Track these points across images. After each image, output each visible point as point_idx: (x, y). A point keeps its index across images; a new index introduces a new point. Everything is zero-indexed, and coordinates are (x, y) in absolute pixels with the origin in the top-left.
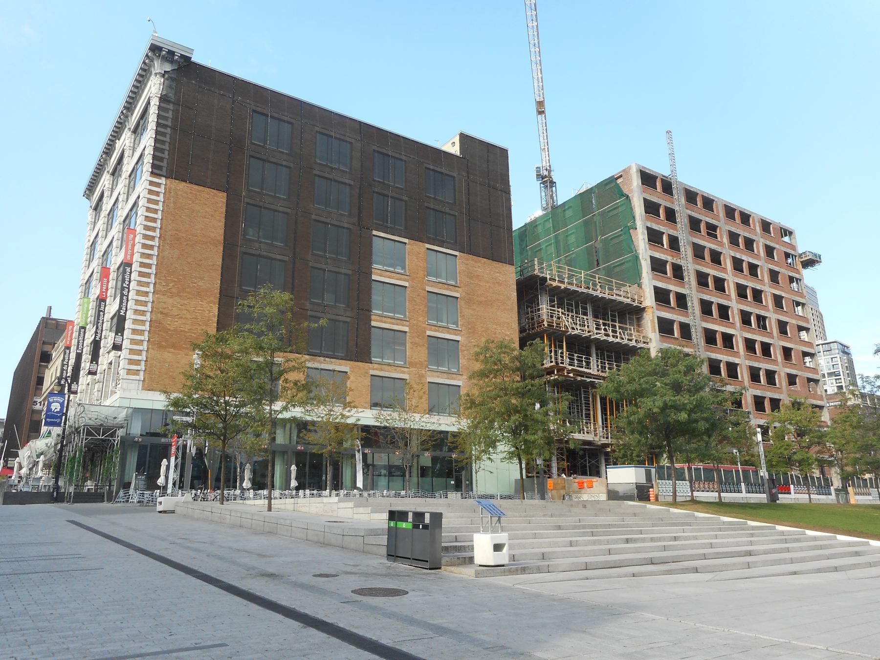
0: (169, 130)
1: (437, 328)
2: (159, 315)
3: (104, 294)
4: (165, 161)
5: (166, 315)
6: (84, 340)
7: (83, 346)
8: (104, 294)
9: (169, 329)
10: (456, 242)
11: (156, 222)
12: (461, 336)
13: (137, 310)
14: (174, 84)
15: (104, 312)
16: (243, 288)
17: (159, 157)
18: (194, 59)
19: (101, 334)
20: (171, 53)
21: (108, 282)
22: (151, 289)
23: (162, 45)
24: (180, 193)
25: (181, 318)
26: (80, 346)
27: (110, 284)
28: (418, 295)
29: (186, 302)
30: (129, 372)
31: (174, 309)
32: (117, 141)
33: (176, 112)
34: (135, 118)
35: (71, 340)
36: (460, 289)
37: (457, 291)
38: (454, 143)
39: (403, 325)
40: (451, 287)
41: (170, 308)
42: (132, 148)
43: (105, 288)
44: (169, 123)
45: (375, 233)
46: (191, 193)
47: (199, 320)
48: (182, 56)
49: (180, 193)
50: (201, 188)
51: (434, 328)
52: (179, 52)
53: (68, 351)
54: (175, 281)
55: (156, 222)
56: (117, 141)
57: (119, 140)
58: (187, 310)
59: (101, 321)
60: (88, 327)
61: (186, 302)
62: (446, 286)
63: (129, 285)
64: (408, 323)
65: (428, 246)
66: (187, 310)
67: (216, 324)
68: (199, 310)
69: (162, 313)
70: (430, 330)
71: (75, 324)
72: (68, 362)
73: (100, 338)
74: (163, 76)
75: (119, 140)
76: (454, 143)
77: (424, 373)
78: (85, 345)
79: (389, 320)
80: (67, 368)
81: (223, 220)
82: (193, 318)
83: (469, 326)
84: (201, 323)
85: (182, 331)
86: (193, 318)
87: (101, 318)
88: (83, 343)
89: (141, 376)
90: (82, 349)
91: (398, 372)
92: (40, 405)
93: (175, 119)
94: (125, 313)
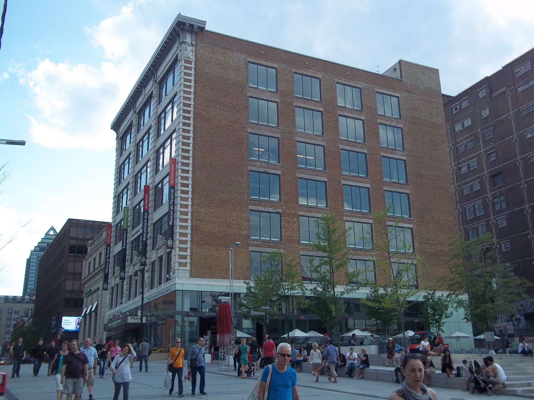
1: (394, 219)
2: (196, 221)
4: (192, 106)
5: (202, 221)
7: (126, 243)
8: (146, 206)
9: (204, 231)
10: (404, 149)
11: (189, 153)
12: (413, 224)
13: (182, 219)
18: (207, 28)
20: (192, 26)
21: (149, 196)
22: (190, 203)
23: (184, 21)
24: (204, 129)
25: (212, 222)
26: (125, 244)
28: (378, 194)
29: (214, 211)
30: (180, 264)
31: (206, 216)
32: (143, 89)
34: (161, 74)
35: (111, 238)
36: (409, 187)
37: (408, 189)
38: (395, 69)
39: (368, 219)
40: (403, 186)
41: (204, 216)
42: (158, 96)
46: (211, 129)
47: (223, 224)
48: (199, 27)
49: (204, 129)
51: (391, 219)
52: (196, 25)
54: (205, 195)
55: (189, 153)
56: (143, 89)
58: (215, 216)
61: (214, 211)
62: (398, 185)
63: (174, 202)
64: (372, 217)
66: (215, 216)
68: (223, 216)
69: (198, 220)
70: (389, 221)
71: (113, 226)
75: (145, 89)
76: (395, 69)
79: (358, 215)
80: (109, 260)
82: (220, 222)
83: (419, 216)
84: (225, 226)
85: (212, 232)
86: (220, 222)
87: (146, 224)
88: (126, 241)
89: (188, 268)
91: (367, 256)
94: (173, 223)
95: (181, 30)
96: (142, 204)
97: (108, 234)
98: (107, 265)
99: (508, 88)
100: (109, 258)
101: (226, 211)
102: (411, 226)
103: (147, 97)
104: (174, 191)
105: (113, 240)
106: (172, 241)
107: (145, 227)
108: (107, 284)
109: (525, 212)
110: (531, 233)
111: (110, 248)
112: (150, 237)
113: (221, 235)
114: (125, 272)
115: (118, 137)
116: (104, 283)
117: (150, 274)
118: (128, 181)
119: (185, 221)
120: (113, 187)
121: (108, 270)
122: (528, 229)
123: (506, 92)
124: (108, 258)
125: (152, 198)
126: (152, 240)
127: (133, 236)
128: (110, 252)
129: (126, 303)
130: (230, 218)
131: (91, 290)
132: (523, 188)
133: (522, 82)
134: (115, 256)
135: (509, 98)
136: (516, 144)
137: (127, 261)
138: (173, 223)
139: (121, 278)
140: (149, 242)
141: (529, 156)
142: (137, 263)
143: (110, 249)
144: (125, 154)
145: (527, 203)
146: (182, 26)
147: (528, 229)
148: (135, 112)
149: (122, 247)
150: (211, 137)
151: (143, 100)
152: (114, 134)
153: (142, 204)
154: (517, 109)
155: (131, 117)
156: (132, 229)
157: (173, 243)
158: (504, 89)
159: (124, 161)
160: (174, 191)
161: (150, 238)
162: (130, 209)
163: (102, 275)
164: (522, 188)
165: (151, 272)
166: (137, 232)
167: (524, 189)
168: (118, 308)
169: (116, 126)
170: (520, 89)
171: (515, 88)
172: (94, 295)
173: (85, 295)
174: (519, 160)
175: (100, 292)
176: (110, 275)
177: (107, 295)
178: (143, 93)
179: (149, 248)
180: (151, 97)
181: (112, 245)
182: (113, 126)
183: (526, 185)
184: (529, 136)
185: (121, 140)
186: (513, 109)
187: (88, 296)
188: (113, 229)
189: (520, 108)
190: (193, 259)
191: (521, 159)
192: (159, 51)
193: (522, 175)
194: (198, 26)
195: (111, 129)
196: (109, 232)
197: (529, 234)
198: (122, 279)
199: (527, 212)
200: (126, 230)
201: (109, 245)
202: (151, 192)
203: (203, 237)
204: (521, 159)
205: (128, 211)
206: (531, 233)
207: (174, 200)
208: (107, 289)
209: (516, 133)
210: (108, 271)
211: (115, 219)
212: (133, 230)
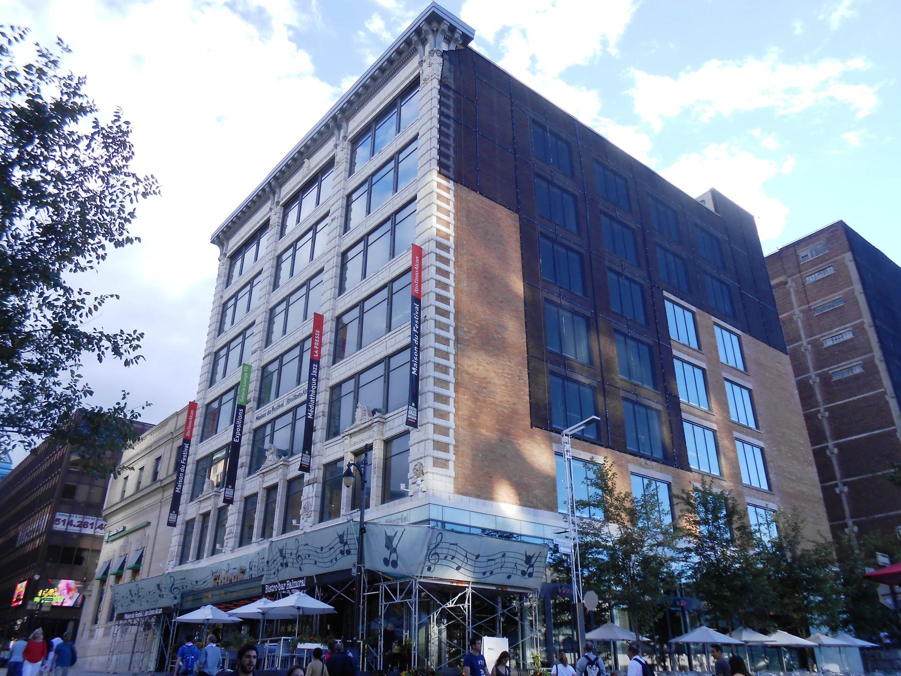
0: (451, 122)
3: (316, 352)
6: (242, 424)
7: (241, 432)
8: (316, 352)
14: (453, 69)
15: (317, 378)
16: (549, 348)
17: (444, 153)
19: (314, 409)
20: (452, 29)
27: (324, 338)
31: (481, 368)
32: (306, 160)
33: (457, 102)
35: (192, 427)
37: (749, 381)
43: (317, 344)
44: (451, 113)
45: (666, 294)
46: (482, 207)
50: (492, 203)
53: (187, 446)
56: (306, 160)
57: (308, 159)
59: (313, 391)
60: (248, 407)
63: (419, 330)
65: (714, 319)
66: (495, 372)
67: (528, 398)
68: (508, 374)
72: (186, 462)
73: (313, 416)
74: (442, 56)
77: (741, 489)
78: (244, 431)
80: (185, 469)
81: (519, 250)
88: (242, 428)
90: (240, 437)
92: (64, 525)
93: (457, 110)
94: (418, 372)
95: (433, 31)
96: (308, 344)
97: (188, 421)
98: (181, 478)
99: (788, 277)
100: (186, 465)
101: (512, 365)
102: (762, 444)
103: (311, 174)
104: (420, 307)
105: (196, 431)
106: (415, 409)
107: (313, 391)
108: (177, 513)
109: (828, 453)
110: (840, 484)
111: (189, 446)
112: (323, 412)
113: (506, 411)
114: (233, 488)
115: (223, 254)
116: (171, 512)
117: (320, 490)
118: (253, 320)
119: (444, 368)
120: (206, 338)
121: (182, 488)
122: (834, 478)
123: (786, 283)
124: (183, 464)
125: (328, 337)
126: (326, 419)
127: (258, 418)
128: (188, 453)
129: (232, 551)
130: (519, 379)
131: (124, 528)
132: (823, 417)
133: (813, 269)
134: (198, 462)
135: (792, 290)
136: (807, 353)
137: (242, 467)
138: (418, 372)
139: (225, 500)
140: (320, 424)
141: (830, 372)
142: (277, 467)
143: (188, 449)
144: (238, 281)
145: (829, 440)
146: (435, 25)
147: (834, 478)
148: (278, 203)
149: (233, 439)
150: (483, 223)
151: (303, 179)
152: (216, 250)
153: (308, 344)
154: (807, 306)
155: (268, 211)
156: (255, 406)
157: (417, 414)
158: (782, 279)
159: (236, 293)
160: (420, 307)
161: (323, 415)
162: (253, 369)
163: (170, 493)
164: (820, 418)
165: (320, 486)
166: (279, 406)
167: (824, 419)
168: (207, 562)
169: (221, 238)
170: (810, 280)
171: (801, 276)
172: (133, 538)
173: (109, 537)
174: (813, 376)
175: (150, 531)
176: (184, 498)
177: (176, 536)
178: (305, 165)
179: (319, 435)
180: (330, 164)
181: (194, 440)
182: (218, 236)
183: (827, 414)
184: (830, 343)
185: (229, 260)
186: (799, 306)
187: (113, 541)
188: (198, 412)
189: (810, 304)
190: (460, 454)
191: (817, 375)
192: (344, 102)
193: (819, 397)
194: (463, 32)
195: (213, 242)
196: (191, 416)
197: (836, 485)
198: (229, 501)
199: (832, 453)
200: (244, 407)
201: (187, 440)
202: (329, 327)
203: (477, 411)
204: (817, 375)
205: (249, 372)
206: (840, 484)
207: (419, 325)
208: (172, 524)
209: (806, 338)
210: (181, 490)
211: (205, 394)
212: (258, 408)
